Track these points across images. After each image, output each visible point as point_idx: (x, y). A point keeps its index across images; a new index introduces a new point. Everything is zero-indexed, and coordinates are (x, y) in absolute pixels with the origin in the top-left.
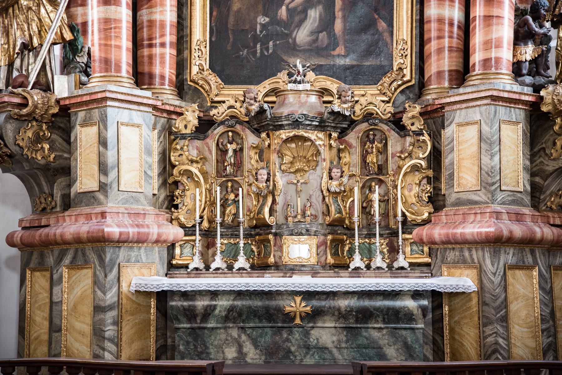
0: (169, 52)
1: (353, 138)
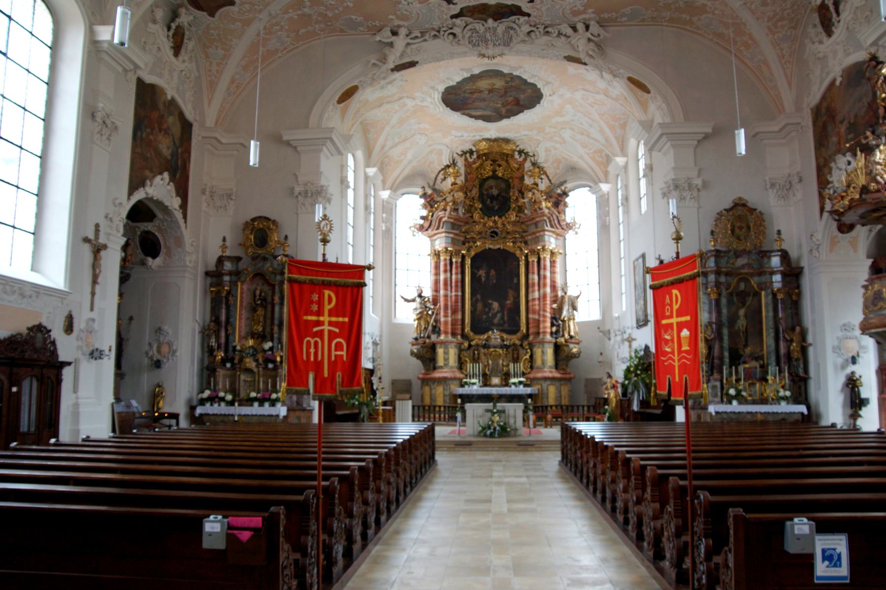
0: (459, 327)
1: (510, 350)
